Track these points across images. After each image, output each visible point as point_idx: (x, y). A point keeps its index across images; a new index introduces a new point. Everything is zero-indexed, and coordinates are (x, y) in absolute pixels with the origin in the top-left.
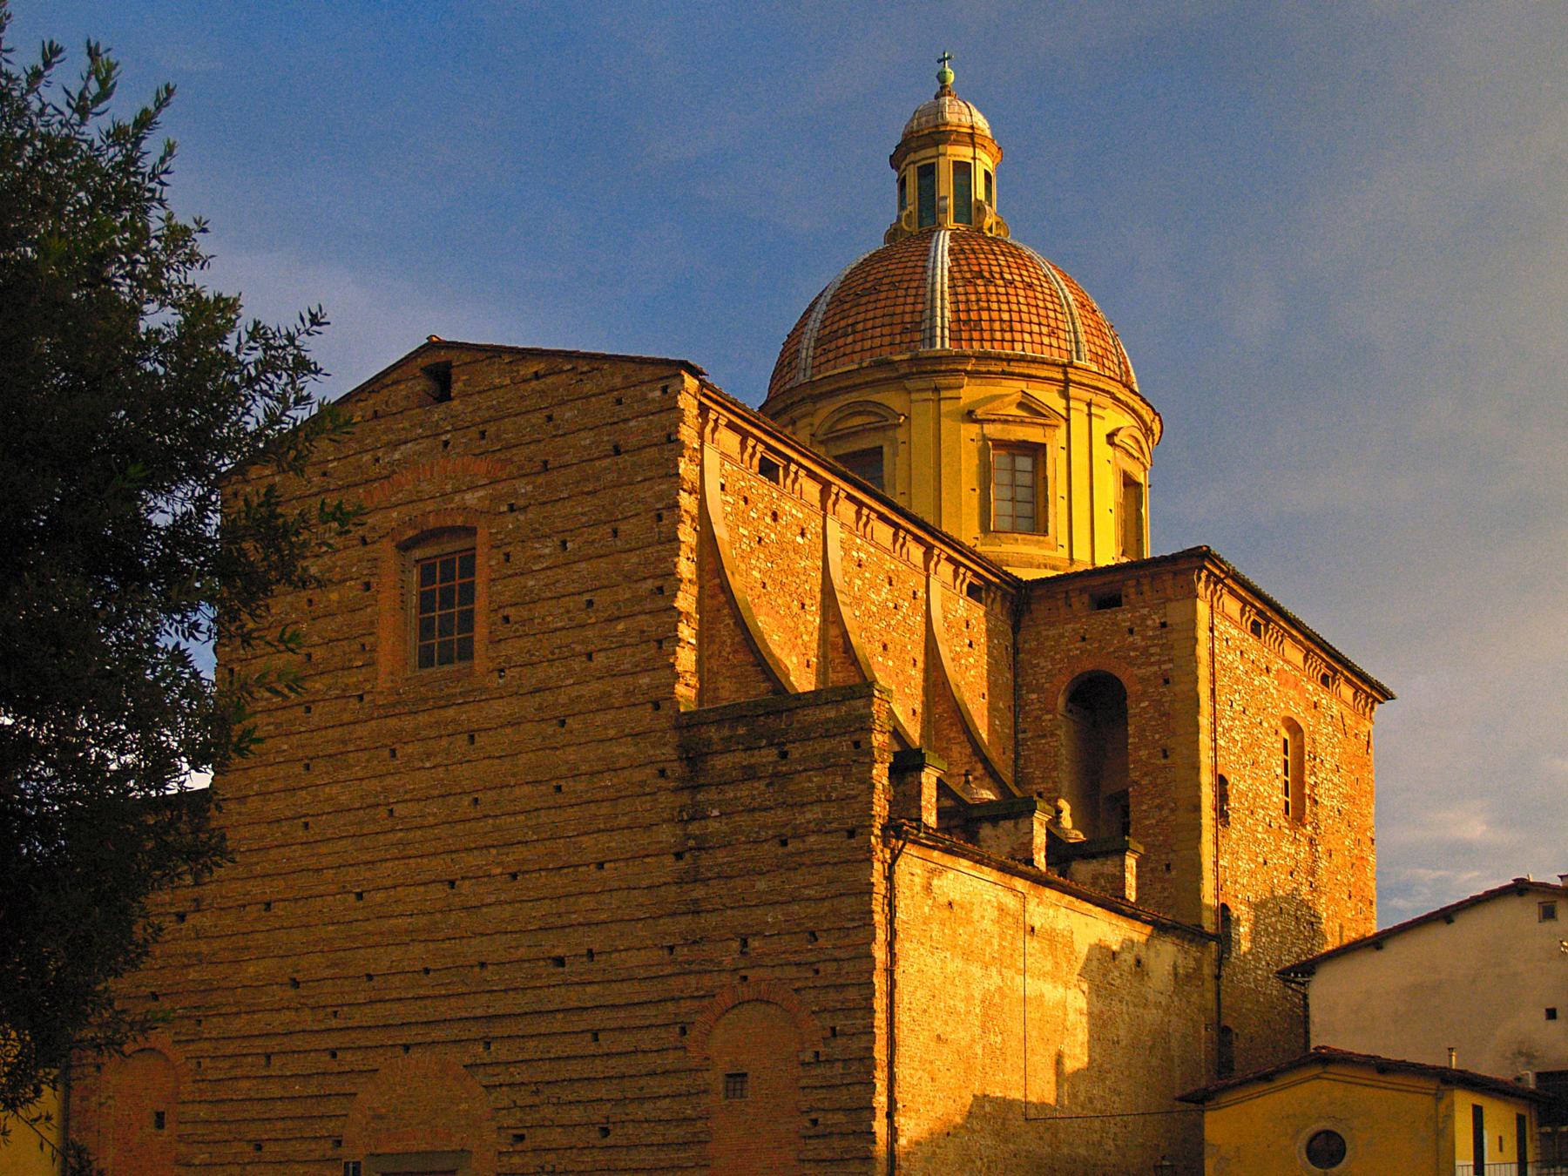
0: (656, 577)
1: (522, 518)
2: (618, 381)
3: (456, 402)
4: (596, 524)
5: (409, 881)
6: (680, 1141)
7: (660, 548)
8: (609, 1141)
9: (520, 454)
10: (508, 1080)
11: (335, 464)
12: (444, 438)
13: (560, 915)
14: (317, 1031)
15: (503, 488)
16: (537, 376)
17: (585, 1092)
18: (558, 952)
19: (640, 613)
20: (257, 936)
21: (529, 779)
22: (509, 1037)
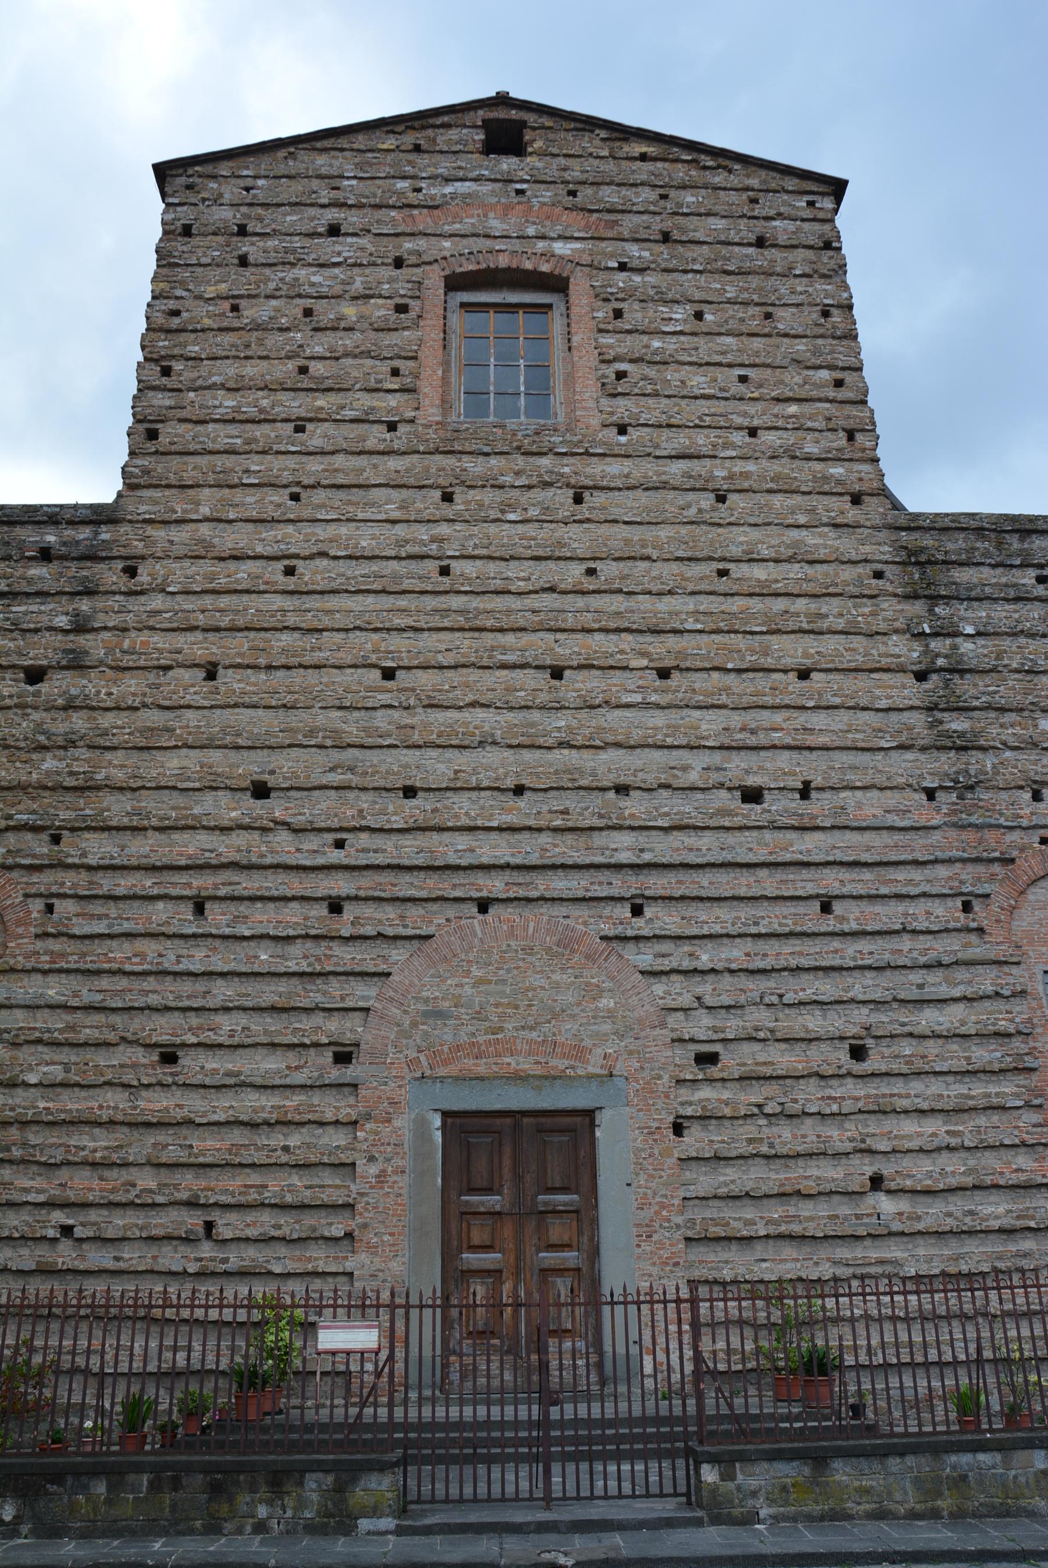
0: (831, 367)
1: (637, 279)
2: (754, 182)
3: (529, 159)
4: (745, 304)
5: (485, 662)
6: (996, 1067)
7: (834, 342)
8: (866, 1066)
9: (628, 223)
10: (686, 964)
11: (354, 182)
12: (518, 186)
13: (753, 732)
14: (304, 868)
15: (608, 247)
16: (643, 157)
17: (826, 988)
18: (752, 781)
19: (820, 400)
20: (189, 714)
21: (680, 553)
22: (683, 898)
